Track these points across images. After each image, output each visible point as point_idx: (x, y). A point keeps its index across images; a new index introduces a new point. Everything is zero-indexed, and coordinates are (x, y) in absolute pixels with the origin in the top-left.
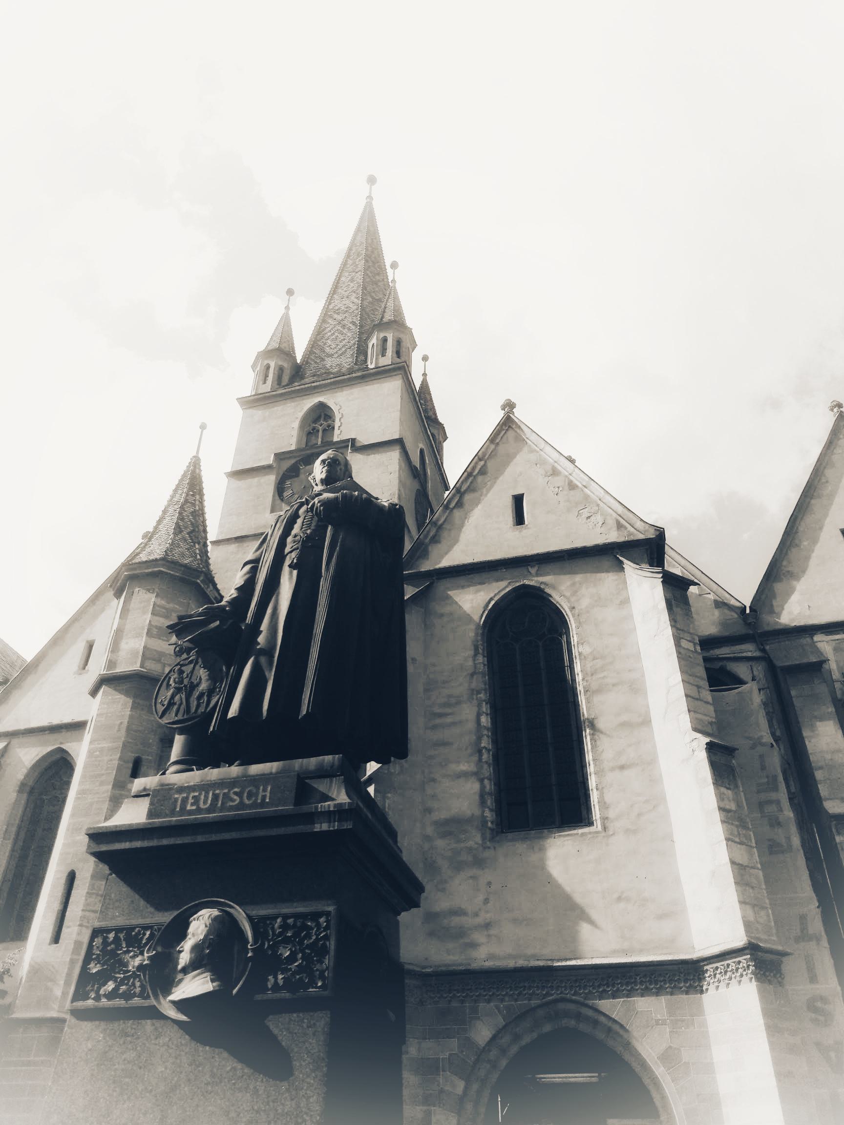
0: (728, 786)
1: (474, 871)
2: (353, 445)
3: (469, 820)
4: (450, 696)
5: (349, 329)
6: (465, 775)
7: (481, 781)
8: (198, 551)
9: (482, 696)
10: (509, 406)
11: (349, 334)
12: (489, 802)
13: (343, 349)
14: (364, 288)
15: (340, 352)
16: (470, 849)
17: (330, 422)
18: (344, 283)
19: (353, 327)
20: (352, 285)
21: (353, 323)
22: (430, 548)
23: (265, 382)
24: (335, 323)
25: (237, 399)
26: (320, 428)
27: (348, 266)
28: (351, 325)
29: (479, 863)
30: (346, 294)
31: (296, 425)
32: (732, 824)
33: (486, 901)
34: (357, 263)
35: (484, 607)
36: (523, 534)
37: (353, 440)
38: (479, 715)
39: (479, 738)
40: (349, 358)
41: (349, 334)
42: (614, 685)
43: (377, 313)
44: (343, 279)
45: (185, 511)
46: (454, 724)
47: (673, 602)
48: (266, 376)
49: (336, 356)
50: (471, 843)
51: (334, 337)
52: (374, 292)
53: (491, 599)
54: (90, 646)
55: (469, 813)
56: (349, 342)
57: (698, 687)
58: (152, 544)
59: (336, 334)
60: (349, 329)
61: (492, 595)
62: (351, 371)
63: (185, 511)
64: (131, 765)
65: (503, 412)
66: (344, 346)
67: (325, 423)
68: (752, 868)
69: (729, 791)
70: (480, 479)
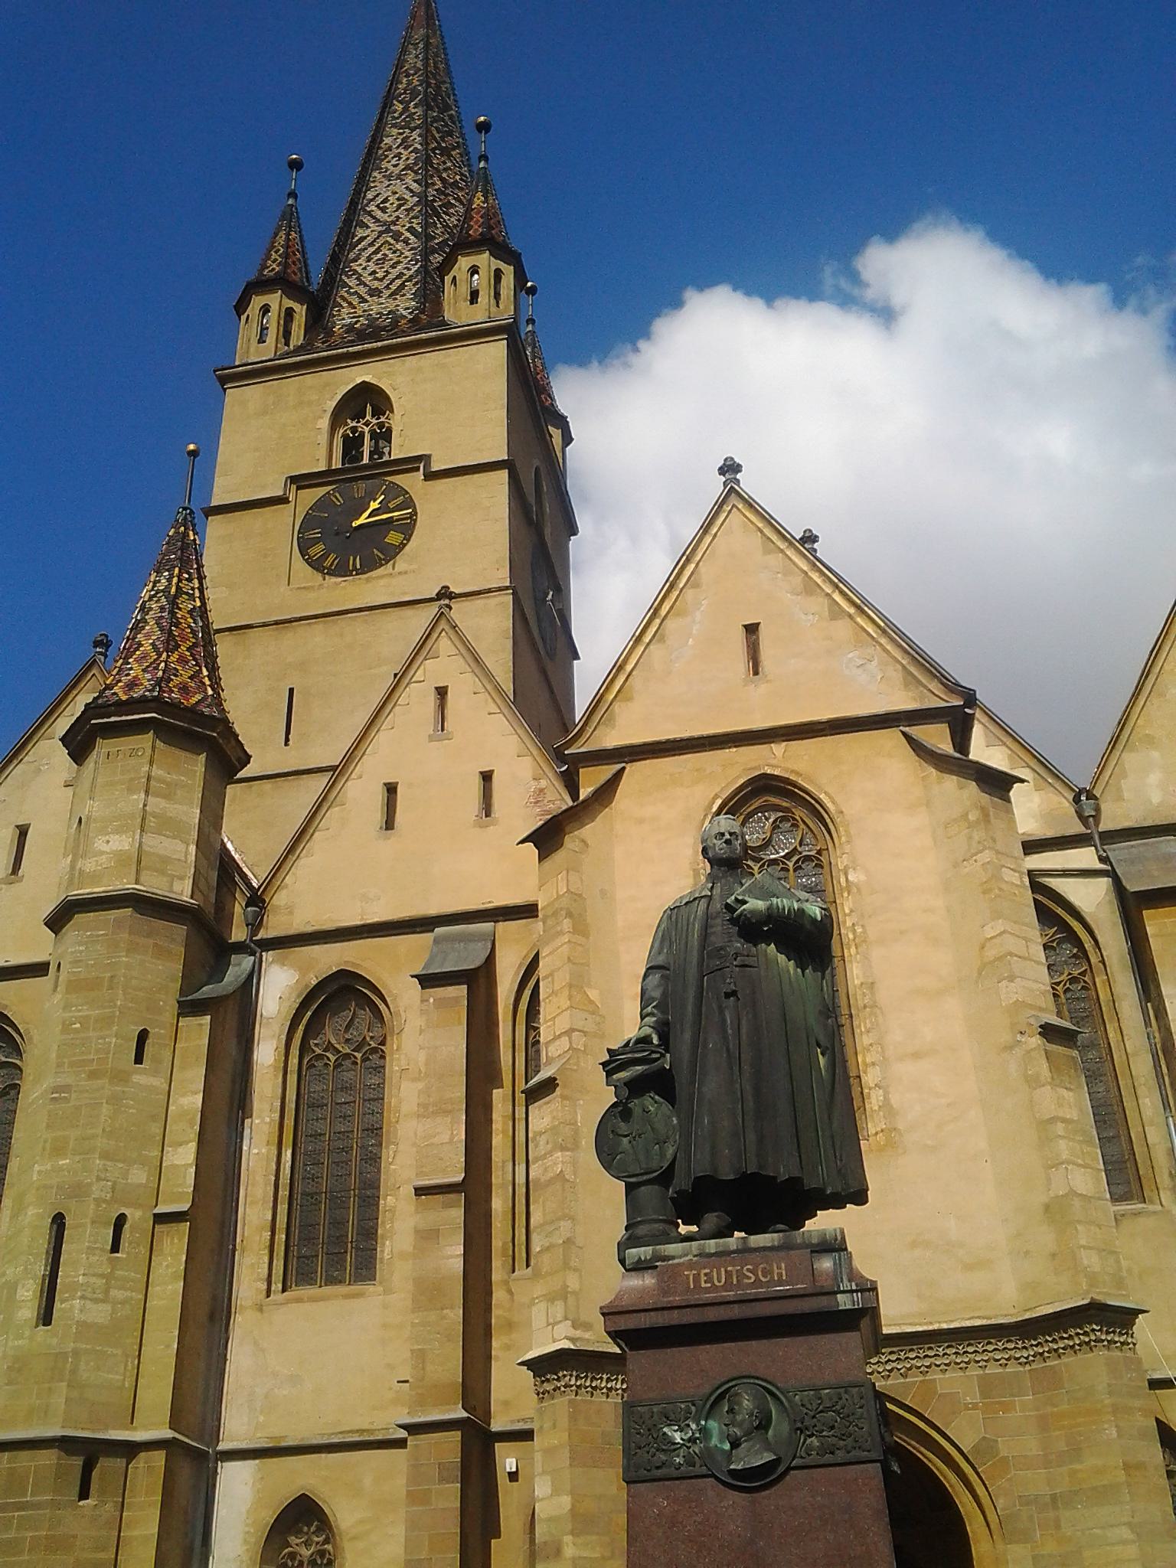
0: (1068, 1086)
2: (427, 465)
5: (406, 242)
8: (208, 682)
10: (730, 468)
11: (407, 253)
13: (398, 282)
14: (428, 161)
15: (393, 287)
17: (383, 419)
18: (390, 149)
20: (405, 153)
21: (411, 230)
22: (616, 706)
23: (261, 341)
24: (380, 229)
26: (367, 429)
27: (396, 115)
28: (408, 235)
30: (397, 171)
31: (324, 423)
32: (1073, 1140)
34: (413, 111)
35: (705, 810)
36: (759, 691)
37: (425, 458)
40: (411, 299)
41: (407, 253)
42: (902, 933)
43: (452, 211)
44: (387, 140)
45: (180, 609)
47: (992, 811)
48: (264, 329)
51: (379, 256)
52: (445, 170)
53: (716, 796)
54: (23, 832)
56: (409, 269)
58: (131, 669)
59: (384, 251)
60: (406, 242)
61: (717, 790)
62: (416, 324)
63: (180, 609)
65: (723, 479)
66: (399, 277)
67: (374, 421)
68: (1100, 1199)
69: (1071, 1094)
70: (689, 594)
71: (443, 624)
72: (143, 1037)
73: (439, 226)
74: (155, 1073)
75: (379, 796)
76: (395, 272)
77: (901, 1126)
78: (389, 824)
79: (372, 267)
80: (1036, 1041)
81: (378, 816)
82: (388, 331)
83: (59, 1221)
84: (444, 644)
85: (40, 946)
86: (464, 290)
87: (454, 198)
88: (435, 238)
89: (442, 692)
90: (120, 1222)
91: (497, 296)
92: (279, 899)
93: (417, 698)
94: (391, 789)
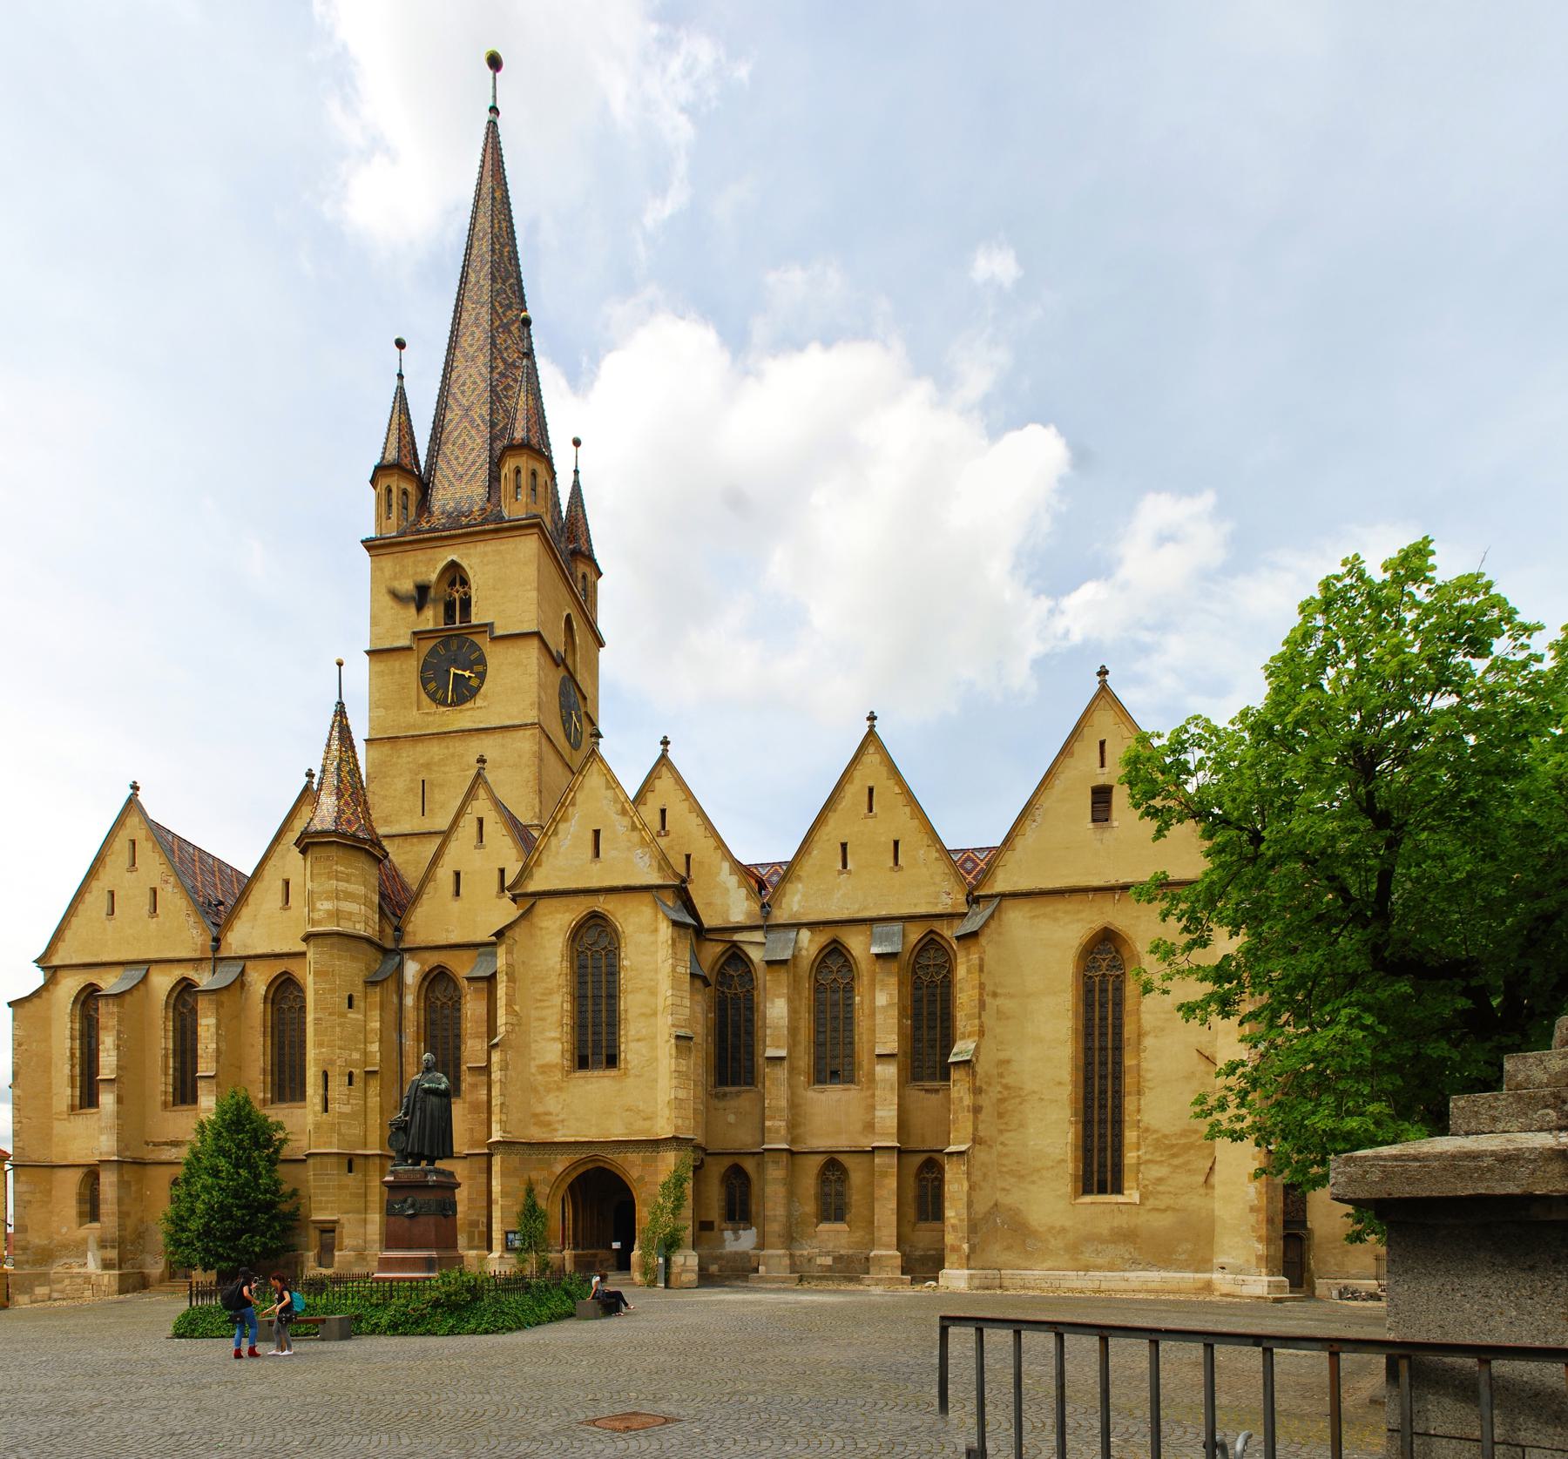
1: (557, 1094)
3: (555, 1066)
4: (547, 988)
6: (554, 1039)
7: (562, 1043)
9: (565, 990)
12: (568, 1056)
13: (474, 468)
16: (555, 1081)
19: (482, 427)
21: (481, 416)
25: (362, 542)
28: (479, 422)
29: (560, 1089)
33: (563, 1109)
38: (562, 1003)
39: (562, 1017)
41: (479, 441)
46: (548, 1007)
48: (390, 506)
49: (466, 479)
50: (556, 1078)
54: (287, 883)
55: (555, 1061)
57: (682, 997)
64: (347, 1001)
66: (473, 463)
71: (480, 780)
72: (350, 998)
73: (501, 411)
74: (358, 1013)
75: (451, 879)
76: (471, 458)
77: (629, 1067)
78: (457, 893)
79: (457, 452)
80: (673, 1041)
81: (451, 888)
82: (466, 517)
83: (325, 1075)
84: (482, 793)
85: (302, 947)
86: (511, 487)
87: (513, 380)
88: (497, 424)
89: (480, 821)
90: (351, 1075)
91: (534, 490)
92: (410, 928)
93: (468, 826)
94: (457, 874)
